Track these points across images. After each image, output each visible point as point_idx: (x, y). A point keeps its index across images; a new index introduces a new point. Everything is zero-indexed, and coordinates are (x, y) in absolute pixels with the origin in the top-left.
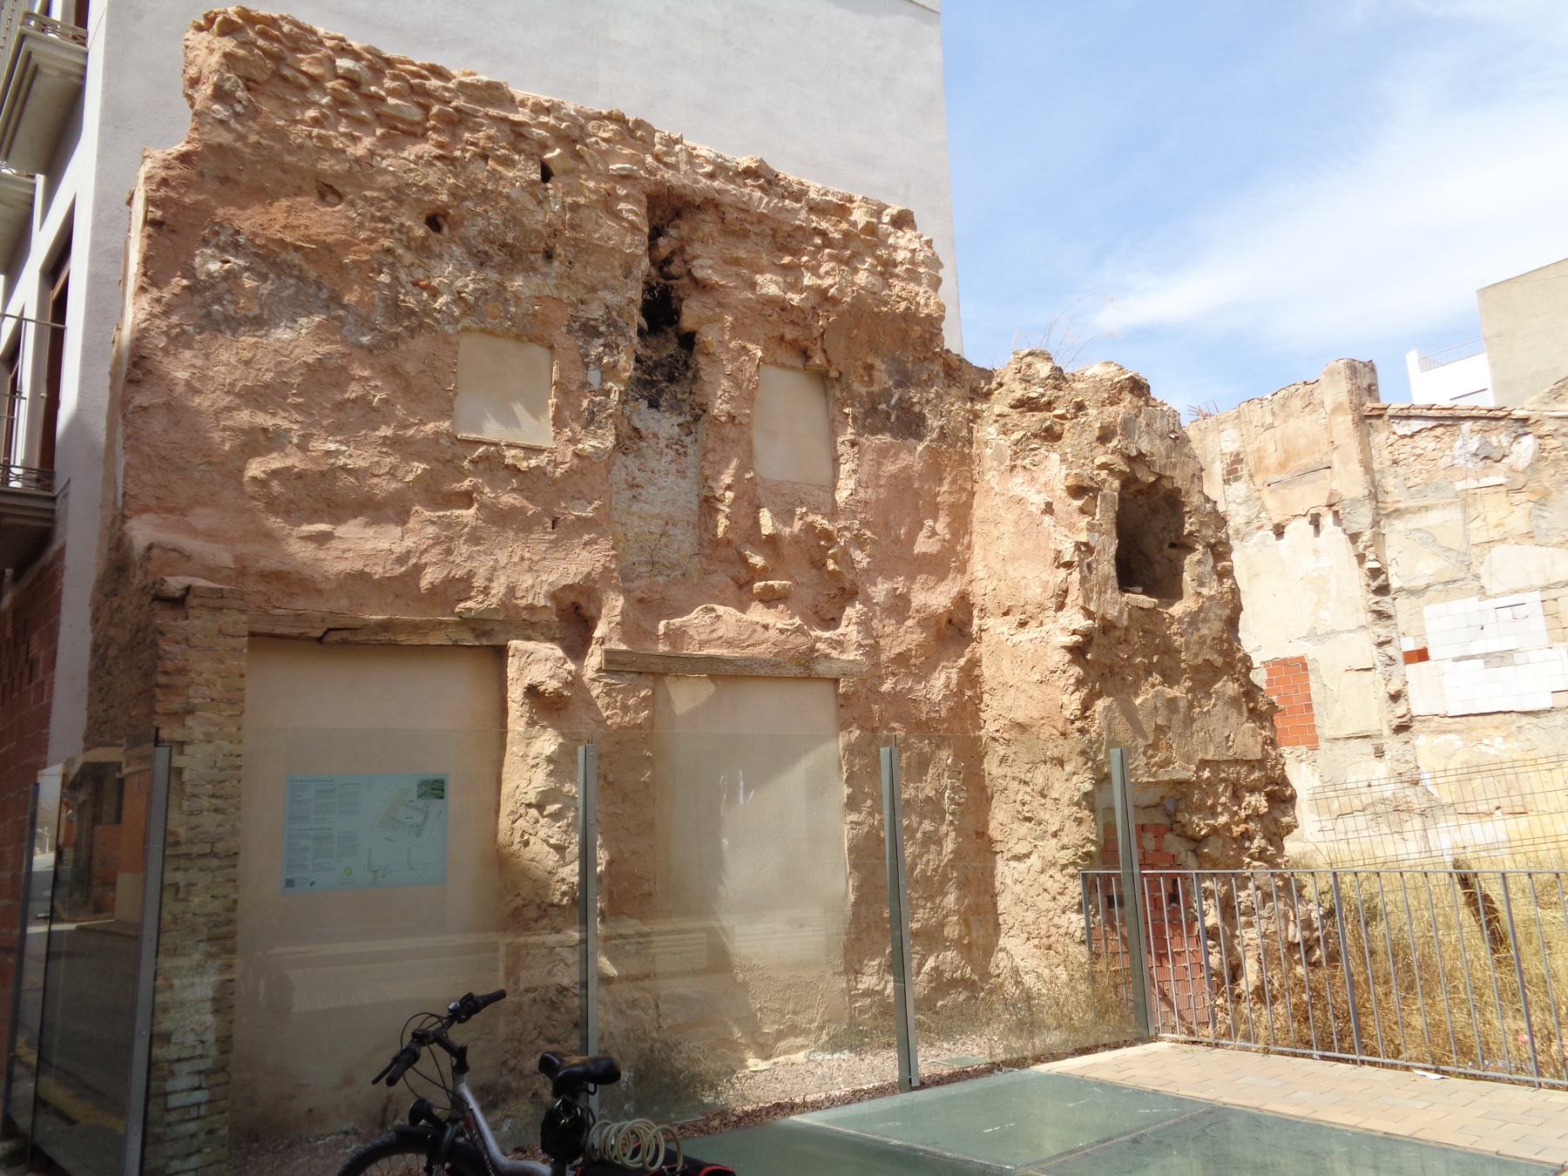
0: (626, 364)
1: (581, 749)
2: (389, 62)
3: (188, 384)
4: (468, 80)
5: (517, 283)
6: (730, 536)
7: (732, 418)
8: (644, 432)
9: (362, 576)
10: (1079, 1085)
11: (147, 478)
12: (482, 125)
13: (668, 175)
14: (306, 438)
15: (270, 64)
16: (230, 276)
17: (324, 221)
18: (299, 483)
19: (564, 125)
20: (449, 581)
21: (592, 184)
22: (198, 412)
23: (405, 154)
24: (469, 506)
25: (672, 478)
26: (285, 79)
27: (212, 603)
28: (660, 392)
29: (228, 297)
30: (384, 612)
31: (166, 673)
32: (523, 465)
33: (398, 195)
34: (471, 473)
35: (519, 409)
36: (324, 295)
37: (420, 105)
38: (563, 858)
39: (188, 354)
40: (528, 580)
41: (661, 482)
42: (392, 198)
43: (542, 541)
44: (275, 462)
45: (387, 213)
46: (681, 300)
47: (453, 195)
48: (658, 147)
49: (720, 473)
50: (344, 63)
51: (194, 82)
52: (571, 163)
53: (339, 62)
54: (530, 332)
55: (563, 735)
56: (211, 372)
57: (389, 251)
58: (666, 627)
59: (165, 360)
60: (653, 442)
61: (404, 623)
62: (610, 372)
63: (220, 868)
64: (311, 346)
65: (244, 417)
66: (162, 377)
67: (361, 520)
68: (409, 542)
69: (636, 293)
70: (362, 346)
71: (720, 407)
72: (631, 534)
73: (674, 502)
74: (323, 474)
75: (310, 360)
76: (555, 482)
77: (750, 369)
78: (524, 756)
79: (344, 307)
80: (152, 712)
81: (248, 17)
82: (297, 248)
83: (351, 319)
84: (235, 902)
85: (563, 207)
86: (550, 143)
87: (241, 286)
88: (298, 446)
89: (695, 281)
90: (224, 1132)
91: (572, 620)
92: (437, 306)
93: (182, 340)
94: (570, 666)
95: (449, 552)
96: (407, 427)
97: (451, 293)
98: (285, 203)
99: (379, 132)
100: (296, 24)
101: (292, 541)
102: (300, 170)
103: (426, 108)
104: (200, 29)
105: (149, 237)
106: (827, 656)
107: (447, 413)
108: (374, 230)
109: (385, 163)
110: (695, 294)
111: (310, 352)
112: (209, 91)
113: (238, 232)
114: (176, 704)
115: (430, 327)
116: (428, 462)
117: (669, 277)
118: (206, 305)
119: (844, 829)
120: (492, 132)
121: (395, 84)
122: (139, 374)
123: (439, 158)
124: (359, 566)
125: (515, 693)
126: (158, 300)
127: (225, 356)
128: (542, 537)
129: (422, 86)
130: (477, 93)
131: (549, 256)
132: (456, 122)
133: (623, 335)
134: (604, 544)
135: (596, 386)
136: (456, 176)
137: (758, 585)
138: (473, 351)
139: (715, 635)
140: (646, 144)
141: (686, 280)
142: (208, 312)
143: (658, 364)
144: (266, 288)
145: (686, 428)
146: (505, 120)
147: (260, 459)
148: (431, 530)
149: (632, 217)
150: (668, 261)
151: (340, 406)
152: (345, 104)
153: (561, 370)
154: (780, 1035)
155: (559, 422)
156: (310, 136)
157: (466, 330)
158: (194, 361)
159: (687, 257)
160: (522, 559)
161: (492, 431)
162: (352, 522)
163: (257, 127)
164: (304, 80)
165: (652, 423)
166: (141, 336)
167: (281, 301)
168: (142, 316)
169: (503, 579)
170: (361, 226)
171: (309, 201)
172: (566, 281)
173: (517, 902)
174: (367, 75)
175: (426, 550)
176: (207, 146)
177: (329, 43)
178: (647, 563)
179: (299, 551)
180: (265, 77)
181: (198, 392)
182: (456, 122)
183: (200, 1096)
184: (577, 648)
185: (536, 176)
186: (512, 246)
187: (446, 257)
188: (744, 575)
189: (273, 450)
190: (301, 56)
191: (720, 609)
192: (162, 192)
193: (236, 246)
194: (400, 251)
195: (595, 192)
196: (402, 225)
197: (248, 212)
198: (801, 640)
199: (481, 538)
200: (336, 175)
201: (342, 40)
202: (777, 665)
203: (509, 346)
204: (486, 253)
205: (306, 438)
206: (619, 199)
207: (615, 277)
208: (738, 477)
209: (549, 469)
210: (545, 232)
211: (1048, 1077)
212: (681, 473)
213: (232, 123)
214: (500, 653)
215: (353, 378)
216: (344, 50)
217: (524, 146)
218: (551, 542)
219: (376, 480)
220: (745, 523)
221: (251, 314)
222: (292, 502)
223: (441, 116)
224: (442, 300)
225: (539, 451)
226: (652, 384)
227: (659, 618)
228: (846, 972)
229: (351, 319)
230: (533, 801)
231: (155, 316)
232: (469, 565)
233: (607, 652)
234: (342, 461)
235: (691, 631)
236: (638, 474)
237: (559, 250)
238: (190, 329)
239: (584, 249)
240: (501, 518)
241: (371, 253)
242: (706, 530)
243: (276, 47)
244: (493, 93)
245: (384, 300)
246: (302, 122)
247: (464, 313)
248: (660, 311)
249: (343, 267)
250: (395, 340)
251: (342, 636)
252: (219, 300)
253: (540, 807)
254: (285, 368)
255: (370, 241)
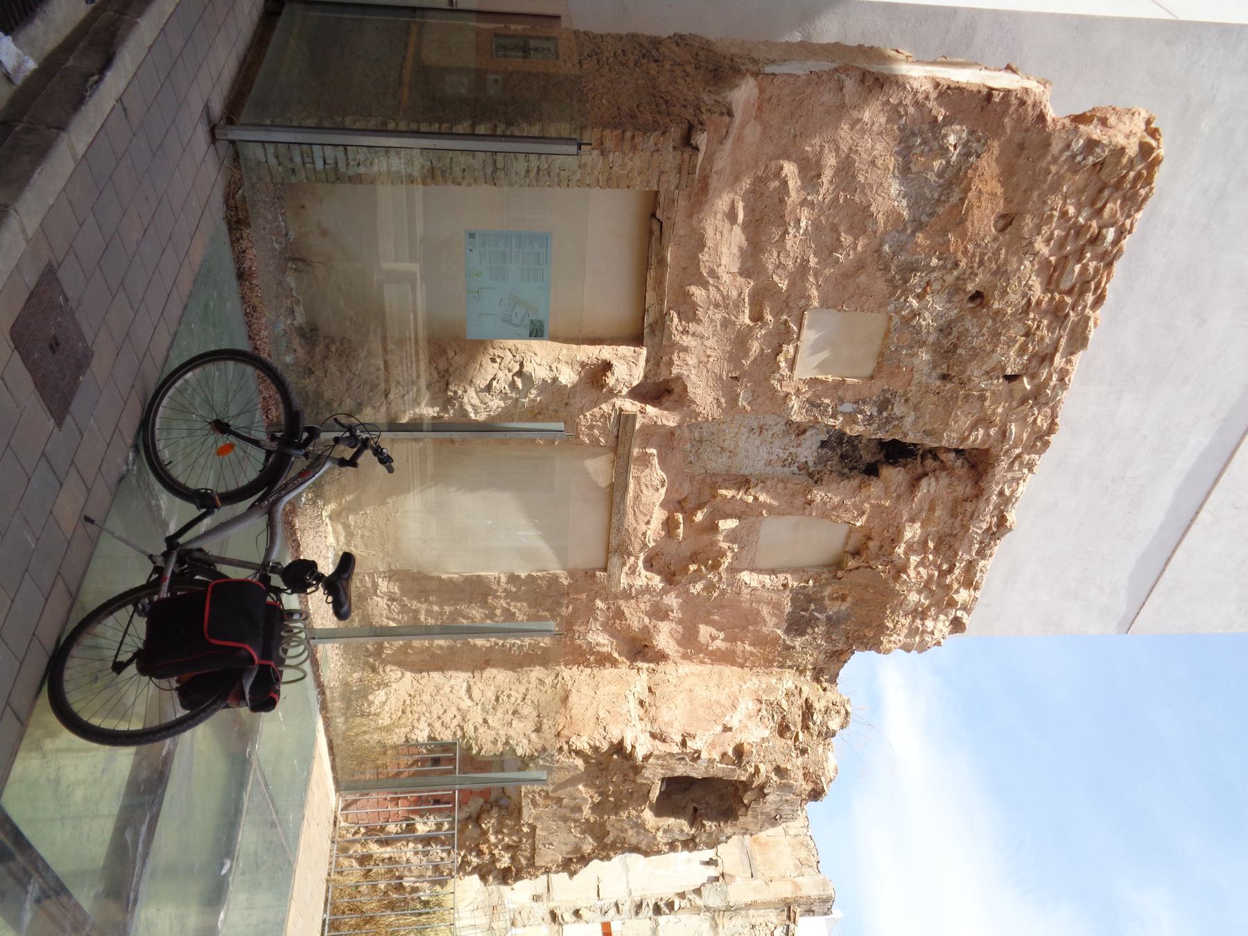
0: (858, 429)
1: (561, 426)
2: (1110, 265)
3: (859, 120)
4: (1091, 323)
5: (925, 356)
6: (719, 498)
7: (810, 503)
8: (802, 437)
9: (701, 245)
10: (307, 759)
11: (787, 90)
12: (1053, 333)
13: (1004, 464)
14: (811, 205)
15: (1113, 181)
16: (944, 151)
17: (983, 219)
18: (776, 200)
19: (1049, 392)
20: (694, 307)
21: (1000, 410)
22: (836, 127)
23: (1034, 278)
24: (751, 319)
25: (766, 456)
26: (1101, 190)
27: (685, 166)
28: (833, 449)
29: (927, 149)
30: (673, 259)
31: (633, 137)
32: (781, 358)
33: (1001, 272)
34: (777, 321)
35: (824, 355)
36: (924, 218)
37: (1073, 288)
38: (482, 391)
39: (883, 120)
40: (692, 360)
41: (763, 449)
42: (998, 268)
43: (721, 370)
44: (794, 184)
45: (987, 264)
46: (905, 466)
47: (998, 312)
48: (1027, 457)
49: (767, 493)
50: (1110, 234)
51: (1104, 122)
52: (1018, 396)
53: (1112, 230)
54: (885, 362)
55: (574, 386)
56: (869, 137)
57: (956, 265)
58: (652, 455)
59: (879, 102)
60: (795, 443)
61: (663, 275)
62: (851, 418)
63: (485, 174)
64: (883, 209)
65: (831, 161)
66: (865, 101)
67: (745, 244)
68: (726, 278)
69: (911, 438)
70: (881, 245)
71: (818, 495)
72: (724, 426)
73: (747, 457)
74: (782, 217)
75: (873, 209)
76: (767, 379)
77: (847, 517)
78: (559, 360)
79: (913, 233)
80: (604, 127)
81: (1153, 165)
82: (962, 200)
83: (903, 238)
84: (459, 184)
85: (983, 390)
86: (1036, 381)
87: (933, 160)
88: (805, 199)
89: (919, 479)
90: (293, 180)
91: (659, 390)
92: (911, 299)
93: (895, 116)
94: (625, 391)
95: (717, 306)
96: (816, 276)
97: (919, 309)
98: (1000, 191)
99: (1053, 259)
100: (1146, 198)
101: (731, 195)
102: (1026, 201)
103: (1070, 292)
104: (1148, 122)
105: (979, 92)
106: (624, 564)
107: (825, 304)
108: (974, 255)
109: (1027, 263)
110: (908, 477)
111: (879, 208)
112: (1095, 137)
113: (978, 156)
114: (609, 143)
115: (894, 294)
116: (788, 290)
117: (923, 458)
118: (921, 133)
119: (494, 572)
120: (1047, 340)
121: (1091, 270)
122: (869, 82)
123: (1029, 301)
124: (709, 243)
125: (606, 352)
126: (927, 98)
127: (879, 147)
128: (724, 370)
129: (1088, 290)
130: (1079, 330)
131: (945, 377)
132: (1057, 314)
133: (879, 429)
134: (717, 413)
135: (840, 408)
136: (1012, 315)
137: (680, 517)
138: (871, 324)
139: (643, 487)
140: (1031, 448)
141: (920, 470)
142: (916, 133)
143: (855, 448)
144: (932, 177)
145: (804, 467)
146: (1056, 350)
147: (796, 172)
148: (734, 294)
149: (972, 438)
150: (935, 458)
151: (835, 229)
152: (1078, 234)
153: (854, 385)
154: (346, 527)
155: (813, 382)
156: (1053, 209)
157: (890, 318)
158: (877, 125)
159: (938, 472)
160: (709, 356)
161: (809, 336)
162: (743, 238)
163: (1062, 171)
164: (1099, 205)
165: (808, 443)
166: (897, 82)
167: (921, 187)
168: (916, 85)
169: (693, 343)
170: (977, 245)
171: (1001, 207)
172: (923, 390)
173: (451, 354)
174: (1100, 250)
175: (719, 290)
176: (1050, 135)
177: (1128, 222)
178: (701, 437)
179: (722, 203)
180: (1103, 177)
181: (852, 128)
182: (1057, 314)
183: (319, 165)
184: (638, 393)
185: (1009, 371)
186: (954, 352)
187: (948, 305)
188: (689, 505)
189: (803, 182)
190: (1119, 202)
191: (663, 491)
192: (1014, 101)
193: (968, 155)
194: (955, 273)
195: (994, 413)
196: (976, 275)
197: (994, 165)
198: (637, 547)
199: (726, 327)
200: (1019, 228)
201: (1130, 232)
202: (619, 530)
203: (875, 347)
204: (950, 334)
205: (811, 205)
206: (987, 429)
207: (925, 424)
208: (764, 505)
209: (778, 376)
210: (964, 377)
211: (314, 730)
212: (769, 463)
213: (1068, 153)
214: (636, 339)
215: (856, 238)
216: (1121, 234)
217: (1034, 362)
218: (721, 376)
219: (775, 254)
220: (728, 508)
221: (912, 165)
222: (762, 195)
223: (1062, 304)
224: (914, 303)
225: (792, 369)
226: (840, 443)
227: (659, 447)
228: (391, 570)
229: (903, 238)
230: (525, 369)
231: (915, 95)
232: (706, 320)
233: (635, 416)
234: (792, 231)
235: (647, 471)
236: (770, 433)
237: (949, 386)
238: (903, 121)
239: (948, 404)
240: (741, 341)
241: (955, 253)
242: (724, 480)
243: (1127, 185)
244: (1079, 340)
245: (917, 261)
246: (1065, 203)
247: (903, 317)
248: (896, 452)
249: (945, 232)
250: (885, 269)
251: (656, 233)
252: (924, 143)
253: (520, 373)
254: (868, 191)
255: (965, 252)
